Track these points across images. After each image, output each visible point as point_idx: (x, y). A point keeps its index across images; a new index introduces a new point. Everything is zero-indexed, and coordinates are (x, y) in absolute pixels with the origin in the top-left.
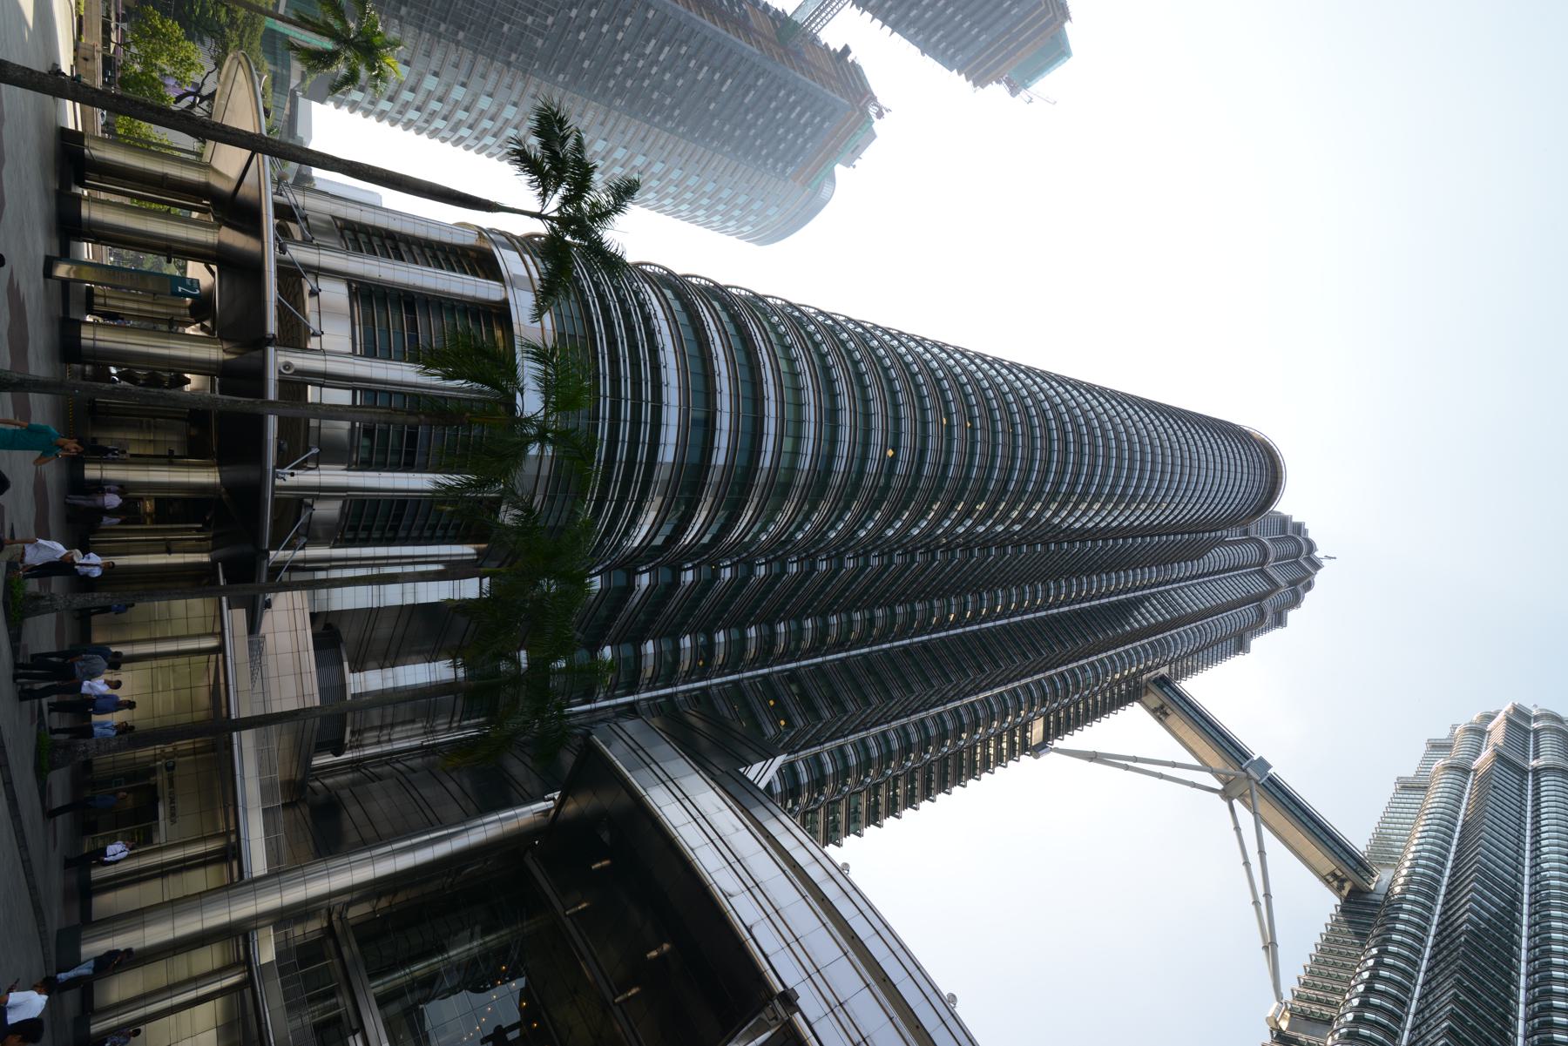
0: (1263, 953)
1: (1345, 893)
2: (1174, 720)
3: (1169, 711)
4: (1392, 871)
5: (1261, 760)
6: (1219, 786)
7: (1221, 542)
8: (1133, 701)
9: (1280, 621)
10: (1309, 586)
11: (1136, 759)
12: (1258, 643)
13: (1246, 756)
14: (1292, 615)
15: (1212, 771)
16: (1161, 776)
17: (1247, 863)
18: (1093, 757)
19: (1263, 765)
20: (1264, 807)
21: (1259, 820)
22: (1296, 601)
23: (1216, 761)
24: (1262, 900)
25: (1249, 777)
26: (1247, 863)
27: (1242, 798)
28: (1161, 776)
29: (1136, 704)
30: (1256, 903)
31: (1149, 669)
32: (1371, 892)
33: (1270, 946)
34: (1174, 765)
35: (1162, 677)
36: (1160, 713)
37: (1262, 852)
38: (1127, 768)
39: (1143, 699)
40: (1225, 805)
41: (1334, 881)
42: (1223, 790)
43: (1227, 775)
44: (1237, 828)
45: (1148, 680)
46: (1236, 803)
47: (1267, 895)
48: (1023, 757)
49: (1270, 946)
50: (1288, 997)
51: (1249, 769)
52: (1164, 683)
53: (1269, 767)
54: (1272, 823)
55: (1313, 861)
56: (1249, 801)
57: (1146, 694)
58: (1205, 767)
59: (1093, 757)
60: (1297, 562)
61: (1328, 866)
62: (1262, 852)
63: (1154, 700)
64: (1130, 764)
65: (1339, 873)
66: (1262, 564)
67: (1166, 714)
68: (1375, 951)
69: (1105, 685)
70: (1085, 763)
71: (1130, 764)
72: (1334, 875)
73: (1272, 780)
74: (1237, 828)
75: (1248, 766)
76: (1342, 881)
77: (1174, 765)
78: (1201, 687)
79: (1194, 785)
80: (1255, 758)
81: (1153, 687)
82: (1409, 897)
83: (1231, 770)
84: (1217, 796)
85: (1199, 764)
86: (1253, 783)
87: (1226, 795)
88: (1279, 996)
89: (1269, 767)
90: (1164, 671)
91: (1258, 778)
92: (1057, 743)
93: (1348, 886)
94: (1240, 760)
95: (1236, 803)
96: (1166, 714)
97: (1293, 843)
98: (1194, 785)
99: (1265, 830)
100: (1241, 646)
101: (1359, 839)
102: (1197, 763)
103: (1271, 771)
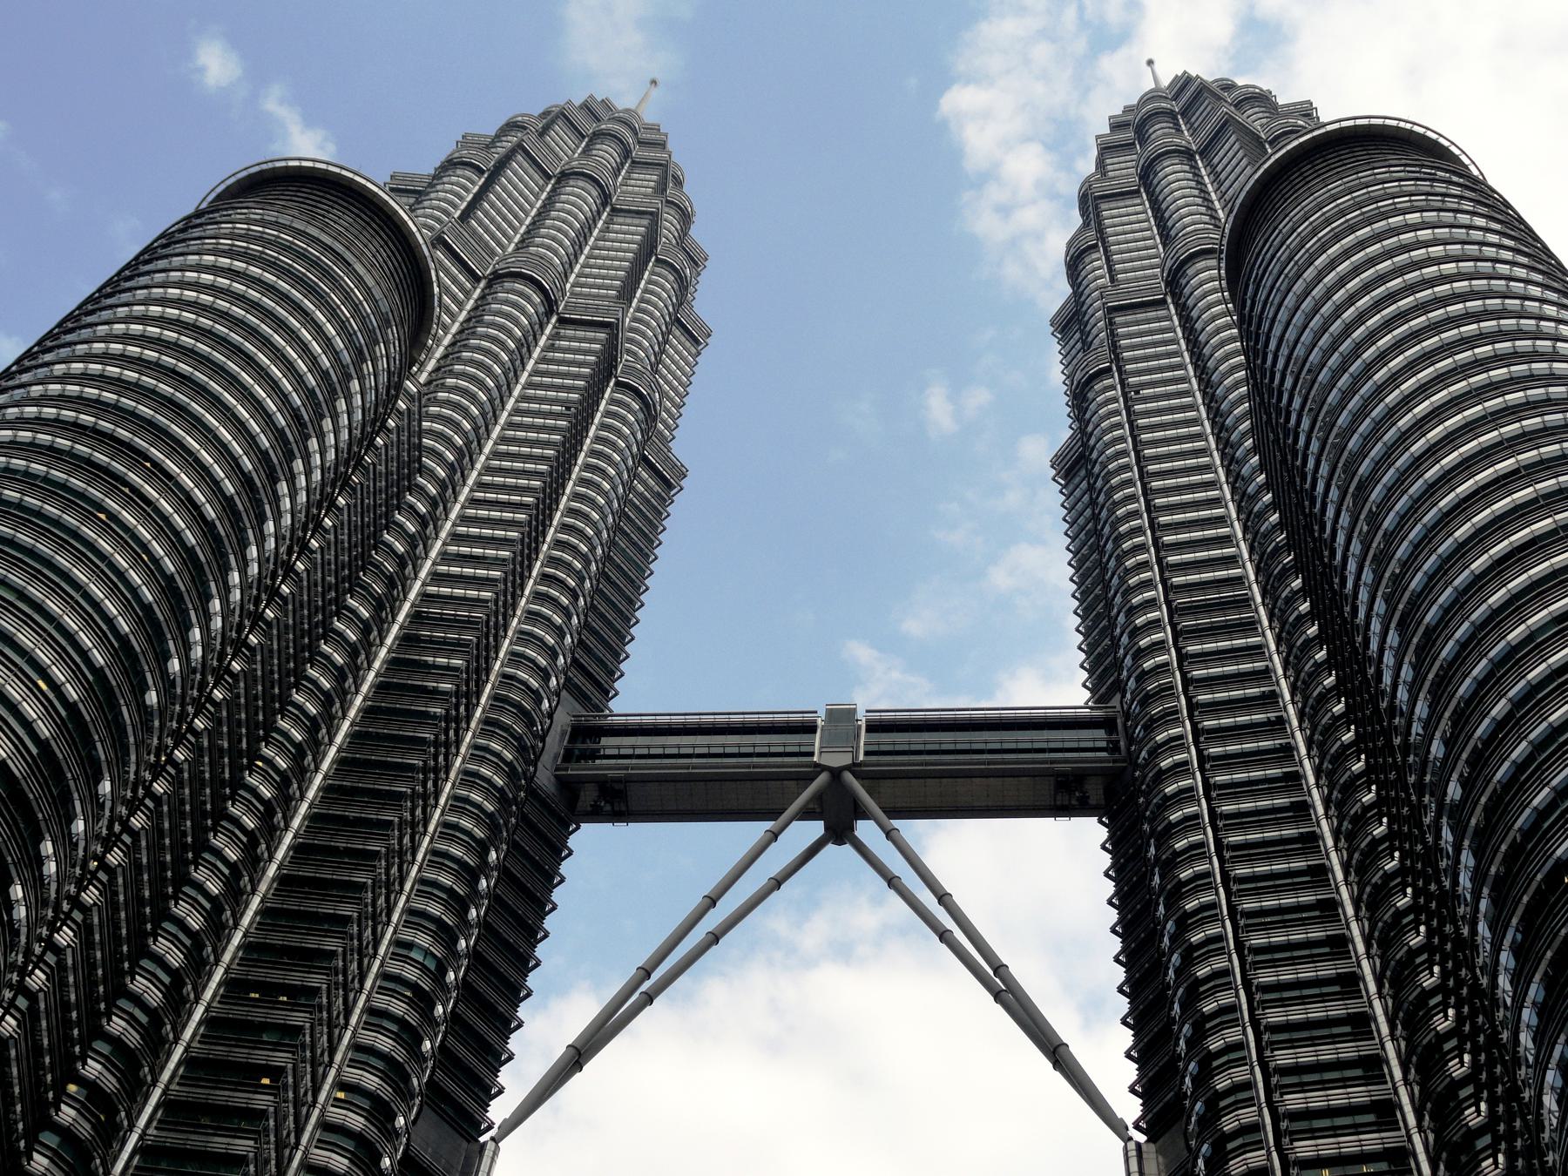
0: (1058, 1074)
6: (816, 829)
7: (413, 418)
11: (646, 972)
16: (715, 938)
19: (841, 716)
25: (836, 773)
30: (998, 996)
38: (649, 999)
40: (847, 848)
79: (777, 883)
80: (822, 714)
86: (848, 777)
94: (804, 749)
98: (777, 883)
103: (861, 716)
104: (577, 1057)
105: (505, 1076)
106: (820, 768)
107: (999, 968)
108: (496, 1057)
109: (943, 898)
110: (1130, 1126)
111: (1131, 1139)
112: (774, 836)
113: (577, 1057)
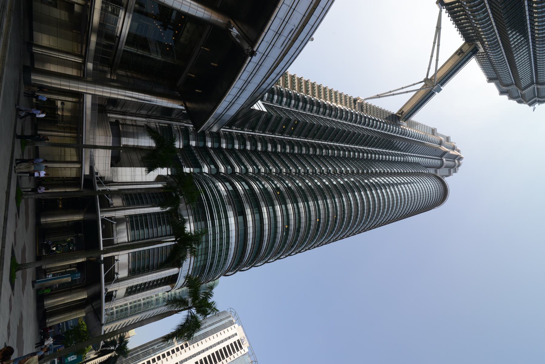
0: (376, 95)
1: (398, 115)
2: (457, 57)
3: (461, 55)
4: (406, 126)
5: (441, 89)
6: (429, 77)
8: (465, 40)
9: (502, 93)
10: (519, 102)
11: (438, 45)
12: (493, 85)
13: (442, 84)
14: (505, 97)
15: (435, 74)
16: (432, 56)
17: (403, 88)
18: (439, 28)
19: (439, 90)
20: (423, 92)
21: (418, 91)
22: (511, 97)
23: (439, 75)
24: (392, 93)
25: (434, 86)
26: (403, 88)
27: (426, 85)
28: (432, 56)
29: (464, 41)
30: (391, 92)
31: (483, 43)
32: (399, 121)
33: (378, 96)
34: (437, 60)
35: (478, 50)
36: (460, 52)
37: (407, 92)
38: (434, 43)
39: (467, 44)
40: (422, 80)
41: (401, 112)
42: (428, 79)
43: (434, 79)
44: (414, 84)
45: (477, 44)
46: (423, 83)
47: (394, 95)
49: (378, 96)
50: (366, 102)
51: (437, 86)
52: (474, 52)
53: (438, 92)
54: (417, 95)
55: (406, 106)
56: (425, 87)
57: (468, 45)
58: (437, 71)
59: (439, 28)
60: (535, 97)
61: (406, 110)
62: (407, 92)
63: (467, 49)
64: (436, 44)
65: (404, 113)
66: (537, 83)
67: (459, 54)
68: (384, 121)
69: (475, 25)
70: (435, 25)
71: (436, 44)
72: (403, 112)
73: (433, 94)
74: (414, 84)
75: (438, 85)
76: (401, 114)
77: (437, 60)
79: (429, 69)
80: (441, 88)
81: (472, 47)
82: (400, 130)
83: (436, 80)
84: (425, 77)
85: (438, 68)
86: (432, 88)
87: (426, 80)
89: (438, 92)
90: (481, 50)
91: (434, 89)
92: (444, 10)
93: (400, 115)
94: (440, 83)
95: (423, 83)
96: (459, 54)
97: (417, 95)
98: (429, 69)
99: (415, 92)
100: (490, 80)
101: (415, 118)
102: (438, 69)
103: (437, 93)
106: (436, 84)
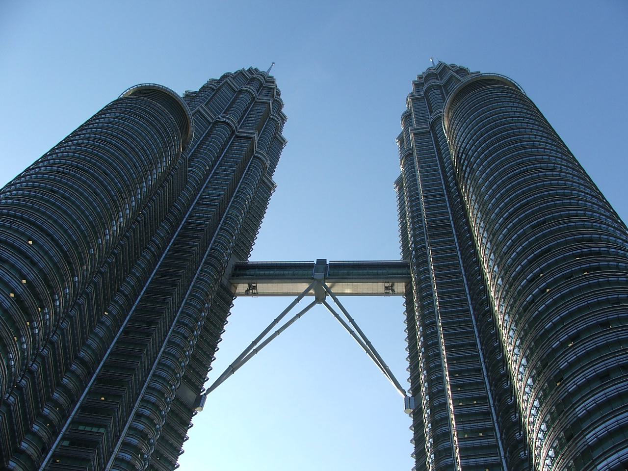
2: (261, 287)
11: (255, 343)
36: (251, 292)
38: (256, 351)
39: (237, 291)
48: (194, 420)
63: (242, 287)
64: (255, 347)
67: (255, 288)
70: (232, 377)
71: (255, 347)
78: (258, 254)
79: (299, 316)
88: (404, 392)
92: (207, 385)
98: (299, 316)
104: (232, 369)
105: (209, 375)
107: (368, 343)
108: (207, 368)
109: (351, 320)
110: (407, 392)
111: (406, 396)
112: (297, 301)
113: (232, 369)
